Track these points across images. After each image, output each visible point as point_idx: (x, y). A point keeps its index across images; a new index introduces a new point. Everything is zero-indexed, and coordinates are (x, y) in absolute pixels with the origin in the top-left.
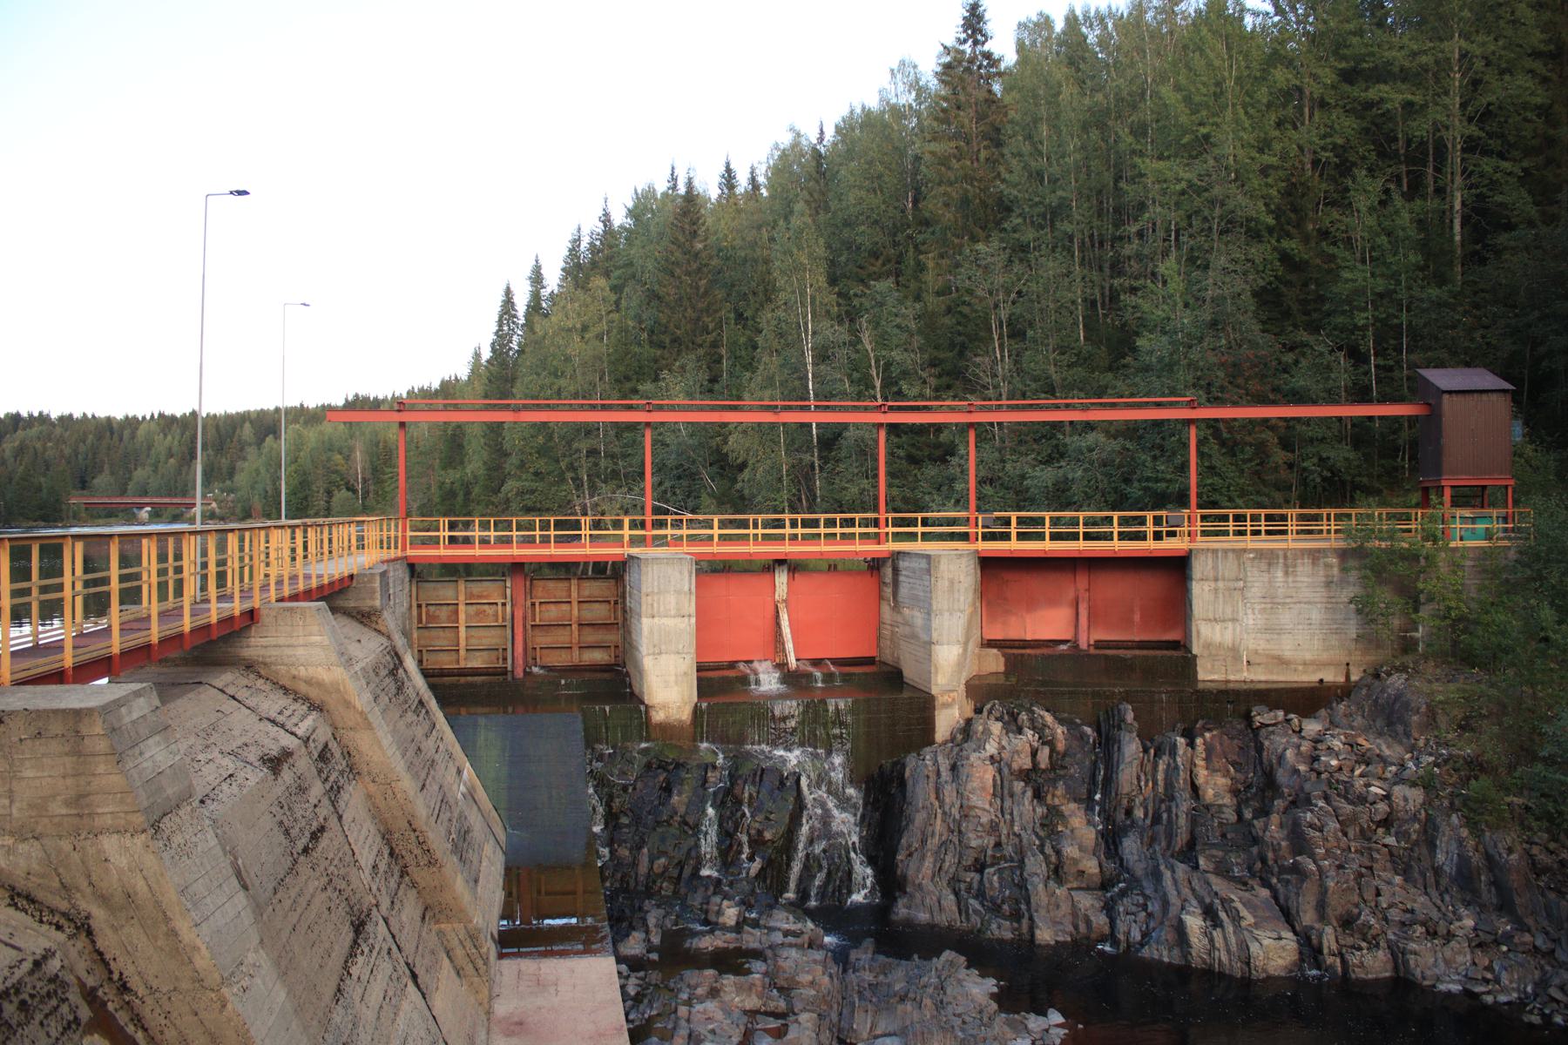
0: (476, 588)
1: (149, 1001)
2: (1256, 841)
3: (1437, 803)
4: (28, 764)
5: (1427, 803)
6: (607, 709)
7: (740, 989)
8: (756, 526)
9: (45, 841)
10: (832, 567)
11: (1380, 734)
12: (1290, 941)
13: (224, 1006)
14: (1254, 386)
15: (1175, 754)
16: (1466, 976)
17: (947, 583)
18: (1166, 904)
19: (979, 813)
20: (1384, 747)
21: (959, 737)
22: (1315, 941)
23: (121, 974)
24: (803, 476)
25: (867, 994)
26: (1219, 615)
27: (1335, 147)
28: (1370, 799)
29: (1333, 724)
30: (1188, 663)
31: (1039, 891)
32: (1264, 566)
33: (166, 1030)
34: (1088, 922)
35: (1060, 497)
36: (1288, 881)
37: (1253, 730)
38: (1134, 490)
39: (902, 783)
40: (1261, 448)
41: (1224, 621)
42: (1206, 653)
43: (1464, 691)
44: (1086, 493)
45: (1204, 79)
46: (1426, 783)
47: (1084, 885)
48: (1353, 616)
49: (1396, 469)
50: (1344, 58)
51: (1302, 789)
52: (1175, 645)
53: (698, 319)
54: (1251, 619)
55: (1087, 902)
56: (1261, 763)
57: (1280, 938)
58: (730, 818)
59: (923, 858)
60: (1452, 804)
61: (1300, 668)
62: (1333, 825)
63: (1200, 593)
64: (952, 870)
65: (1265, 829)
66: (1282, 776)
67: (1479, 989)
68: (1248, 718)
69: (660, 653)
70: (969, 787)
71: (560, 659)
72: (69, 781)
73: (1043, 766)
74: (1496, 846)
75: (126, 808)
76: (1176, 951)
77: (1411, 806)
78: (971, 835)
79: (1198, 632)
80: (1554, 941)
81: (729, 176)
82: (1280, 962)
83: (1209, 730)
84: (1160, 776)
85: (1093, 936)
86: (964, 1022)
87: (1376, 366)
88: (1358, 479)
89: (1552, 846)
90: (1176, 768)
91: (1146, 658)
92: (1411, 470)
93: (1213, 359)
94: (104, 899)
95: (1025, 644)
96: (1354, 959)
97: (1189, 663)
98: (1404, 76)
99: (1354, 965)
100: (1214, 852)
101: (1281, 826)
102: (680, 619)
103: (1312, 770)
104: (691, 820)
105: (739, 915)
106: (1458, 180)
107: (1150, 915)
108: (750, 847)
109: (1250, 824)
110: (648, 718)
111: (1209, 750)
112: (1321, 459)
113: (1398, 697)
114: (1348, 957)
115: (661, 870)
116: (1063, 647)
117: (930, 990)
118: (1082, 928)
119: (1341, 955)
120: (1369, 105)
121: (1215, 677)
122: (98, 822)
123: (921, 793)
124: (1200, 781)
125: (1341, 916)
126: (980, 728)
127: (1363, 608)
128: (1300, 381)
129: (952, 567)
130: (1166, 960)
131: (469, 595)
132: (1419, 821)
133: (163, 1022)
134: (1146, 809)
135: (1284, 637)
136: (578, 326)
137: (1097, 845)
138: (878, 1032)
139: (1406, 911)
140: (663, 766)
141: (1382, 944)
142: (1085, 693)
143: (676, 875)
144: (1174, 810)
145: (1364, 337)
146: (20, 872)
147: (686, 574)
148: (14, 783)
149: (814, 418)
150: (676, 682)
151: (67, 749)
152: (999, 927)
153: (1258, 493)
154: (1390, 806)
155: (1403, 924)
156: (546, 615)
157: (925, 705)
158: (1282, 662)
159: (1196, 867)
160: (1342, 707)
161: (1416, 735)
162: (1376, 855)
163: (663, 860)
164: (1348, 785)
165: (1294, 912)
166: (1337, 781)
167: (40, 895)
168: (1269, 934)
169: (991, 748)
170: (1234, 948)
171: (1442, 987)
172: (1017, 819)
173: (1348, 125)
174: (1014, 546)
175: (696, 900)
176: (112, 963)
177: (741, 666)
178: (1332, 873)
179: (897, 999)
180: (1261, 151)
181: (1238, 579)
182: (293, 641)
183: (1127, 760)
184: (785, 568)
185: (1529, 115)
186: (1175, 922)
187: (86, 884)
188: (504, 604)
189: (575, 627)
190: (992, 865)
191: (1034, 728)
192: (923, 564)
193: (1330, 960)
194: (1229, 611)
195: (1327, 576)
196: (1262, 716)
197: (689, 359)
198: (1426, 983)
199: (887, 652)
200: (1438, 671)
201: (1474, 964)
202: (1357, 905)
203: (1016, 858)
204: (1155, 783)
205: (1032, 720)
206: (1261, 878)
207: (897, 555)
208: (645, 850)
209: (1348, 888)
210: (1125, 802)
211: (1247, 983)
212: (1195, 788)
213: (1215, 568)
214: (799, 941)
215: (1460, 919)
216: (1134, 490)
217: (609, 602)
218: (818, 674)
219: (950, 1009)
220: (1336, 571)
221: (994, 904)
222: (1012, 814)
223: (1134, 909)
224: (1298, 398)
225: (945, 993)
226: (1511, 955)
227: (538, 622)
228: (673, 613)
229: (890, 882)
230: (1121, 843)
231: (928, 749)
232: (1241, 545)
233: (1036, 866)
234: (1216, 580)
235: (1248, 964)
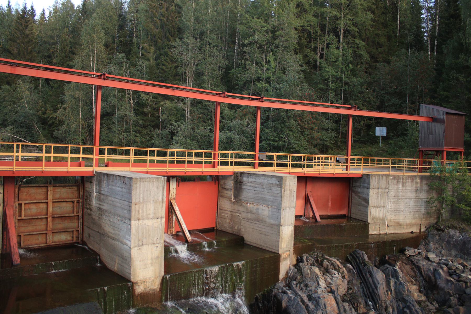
6: (106, 288)
17: (288, 192)
32: (395, 183)
41: (380, 207)
48: (423, 204)
61: (405, 227)
63: (373, 195)
71: (38, 242)
79: (370, 213)
90: (401, 283)
97: (366, 226)
102: (155, 220)
135: (401, 213)
142: (342, 246)
147: (161, 189)
150: (152, 264)
156: (29, 212)
158: (399, 225)
181: (386, 188)
184: (175, 179)
191: (335, 269)
192: (274, 181)
195: (416, 187)
213: (378, 183)
217: (73, 202)
218: (205, 244)
220: (419, 185)
227: (23, 217)
228: (152, 216)
232: (388, 173)
234: (378, 189)
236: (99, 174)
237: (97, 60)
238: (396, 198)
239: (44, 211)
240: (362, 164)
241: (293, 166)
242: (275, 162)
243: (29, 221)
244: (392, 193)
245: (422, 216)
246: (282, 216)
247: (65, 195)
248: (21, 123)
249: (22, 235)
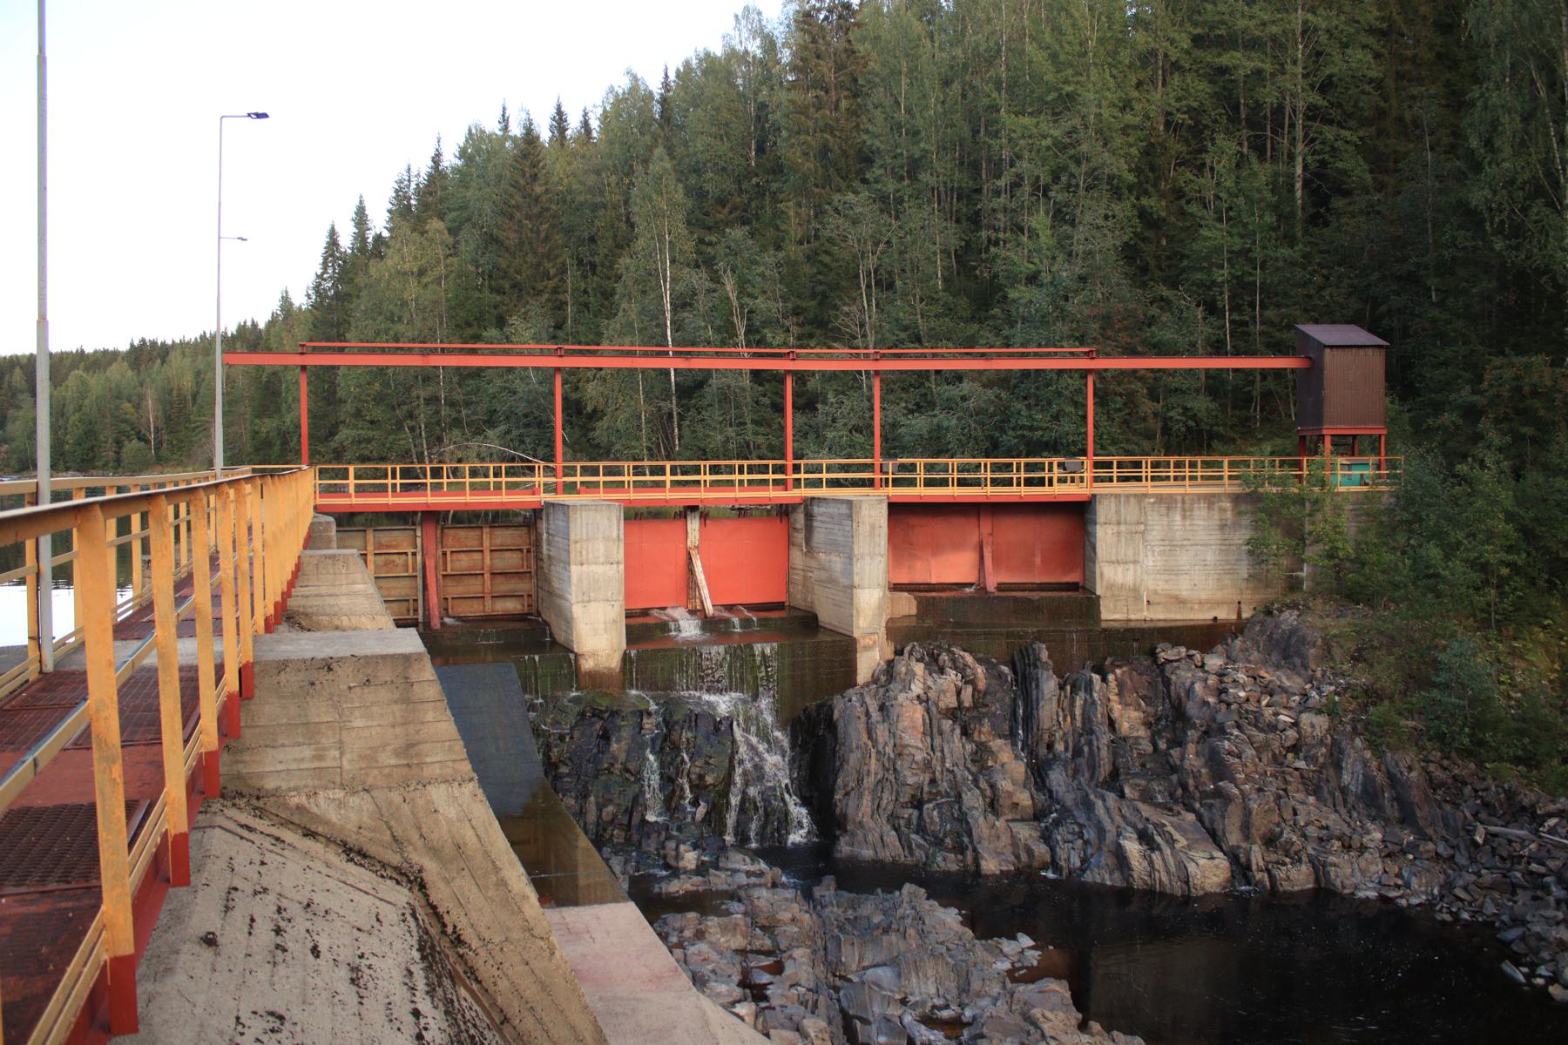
0: (385, 538)
1: (482, 952)
2: (1174, 769)
3: (1340, 728)
4: (357, 713)
5: (1332, 729)
6: (537, 658)
7: (724, 930)
8: (741, 472)
9: (375, 793)
10: (742, 512)
11: (1278, 667)
12: (1222, 862)
13: (553, 954)
14: (1123, 338)
15: (1091, 690)
16: (1380, 883)
17: (868, 528)
18: (1101, 831)
19: (913, 751)
20: (1284, 679)
21: (883, 678)
22: (1243, 860)
23: (455, 927)
24: (662, 422)
25: (848, 927)
26: (1121, 556)
27: (1190, 110)
28: (1281, 726)
29: (1230, 659)
30: (1091, 604)
31: (981, 824)
32: (1163, 511)
33: (499, 982)
34: (1029, 851)
35: (936, 445)
36: (1211, 806)
37: (1158, 666)
38: (1009, 438)
39: (832, 726)
40: (1131, 399)
41: (1126, 563)
42: (1108, 595)
43: (1355, 625)
44: (960, 440)
45: (1071, 38)
46: (1330, 711)
47: (1018, 817)
48: (1244, 557)
49: (1247, 419)
50: (1196, 25)
51: (1214, 720)
52: (1073, 587)
53: (539, 264)
54: (1151, 561)
55: (1025, 832)
56: (1169, 696)
57: (1212, 858)
58: (670, 764)
59: (861, 797)
60: (1354, 729)
61: (1196, 607)
62: (1250, 752)
63: (1105, 536)
64: (890, 807)
65: (1182, 758)
66: (1192, 709)
67: (1392, 894)
68: (1152, 654)
69: (589, 601)
70: (900, 726)
71: (473, 609)
72: (398, 730)
73: (966, 704)
74: (1397, 765)
75: (454, 757)
76: (1117, 875)
77: (1317, 732)
78: (907, 773)
79: (1102, 574)
80: (1453, 847)
81: (561, 118)
82: (1215, 879)
83: (1119, 667)
84: (1078, 712)
85: (1035, 864)
86: (948, 949)
87: (1231, 322)
88: (1215, 428)
89: (1445, 763)
90: (1094, 702)
91: (1053, 599)
92: (1262, 421)
93: (1086, 312)
94: (435, 851)
95: (930, 587)
96: (1280, 873)
97: (1092, 603)
98: (1253, 44)
99: (1281, 879)
100: (1138, 781)
101: (1197, 754)
102: (608, 567)
103: (1221, 701)
104: (632, 766)
105: (698, 859)
106: (1300, 147)
107: (1086, 842)
108: (691, 791)
109: (1166, 754)
110: (578, 666)
111: (1121, 685)
112: (1186, 409)
113: (1293, 632)
114: (1275, 872)
115: (610, 818)
116: (968, 590)
117: (909, 921)
118: (1024, 857)
119: (1269, 872)
120: (1223, 71)
121: (1117, 616)
122: (427, 772)
123: (854, 734)
124: (1116, 715)
125: (1265, 834)
126: (903, 669)
127: (1256, 550)
128: (1167, 335)
129: (872, 512)
130: (1108, 883)
131: (378, 545)
132: (1326, 746)
133: (496, 973)
134: (1066, 743)
135: (1181, 577)
136: (415, 270)
137: (1027, 778)
138: (866, 963)
139: (1322, 828)
140: (597, 714)
141: (1304, 858)
143: (626, 822)
144: (1095, 743)
145: (1221, 293)
146: (351, 827)
147: (615, 521)
148: (344, 732)
149: (672, 364)
150: (605, 630)
151: (396, 696)
152: (944, 860)
153: (1128, 441)
154: (1299, 732)
155: (1321, 839)
156: (457, 565)
157: (846, 648)
158: (1180, 601)
159: (1122, 796)
160: (1238, 642)
161: (1313, 667)
162: (1289, 778)
163: (611, 808)
164: (1258, 715)
165: (1220, 833)
166: (1247, 711)
167: (372, 850)
168: (1202, 854)
169: (917, 688)
170: (1173, 869)
171: (1361, 894)
172: (948, 755)
173: (1202, 88)
174: (920, 492)
175: (651, 846)
176: (445, 916)
177: (655, 613)
178: (1254, 796)
179: (880, 931)
180: (1123, 109)
181: (1139, 523)
182: (336, 590)
183: (1047, 697)
185: (1367, 88)
186: (1112, 848)
187: (417, 837)
188: (414, 554)
189: (487, 576)
190: (930, 801)
191: (956, 668)
192: (844, 509)
193: (1258, 876)
194: (1130, 553)
195: (1221, 520)
196: (1166, 653)
197: (535, 306)
198: (1346, 891)
199: (799, 596)
200: (1327, 607)
201: (1386, 872)
202: (1278, 825)
203: (952, 794)
204: (1073, 718)
205: (954, 661)
206: (1185, 805)
207: (809, 502)
208: (592, 799)
209: (1269, 809)
210: (1046, 737)
211: (1187, 900)
212: (1112, 724)
213: (1118, 512)
214: (762, 881)
215: (1368, 833)
216: (1009, 438)
217: (521, 550)
218: (736, 620)
219: (932, 937)
220: (1229, 515)
221: (936, 837)
222: (942, 751)
223: (1070, 837)
224: (1160, 350)
225: (924, 923)
226: (1417, 862)
227: (449, 572)
228: (601, 560)
229: (829, 821)
230: (1047, 775)
231: (851, 691)
232: (1143, 490)
233: (973, 800)
234: (1119, 523)
235: (1187, 883)
236: (550, 505)
237: (673, 261)
238: (1167, 543)
239: (480, 563)
240: (1226, 473)
241: (995, 482)
242: (921, 475)
243: (459, 577)
244: (1154, 533)
245: (1244, 584)
246: (855, 570)
247: (509, 541)
248: (526, 416)
249: (449, 597)
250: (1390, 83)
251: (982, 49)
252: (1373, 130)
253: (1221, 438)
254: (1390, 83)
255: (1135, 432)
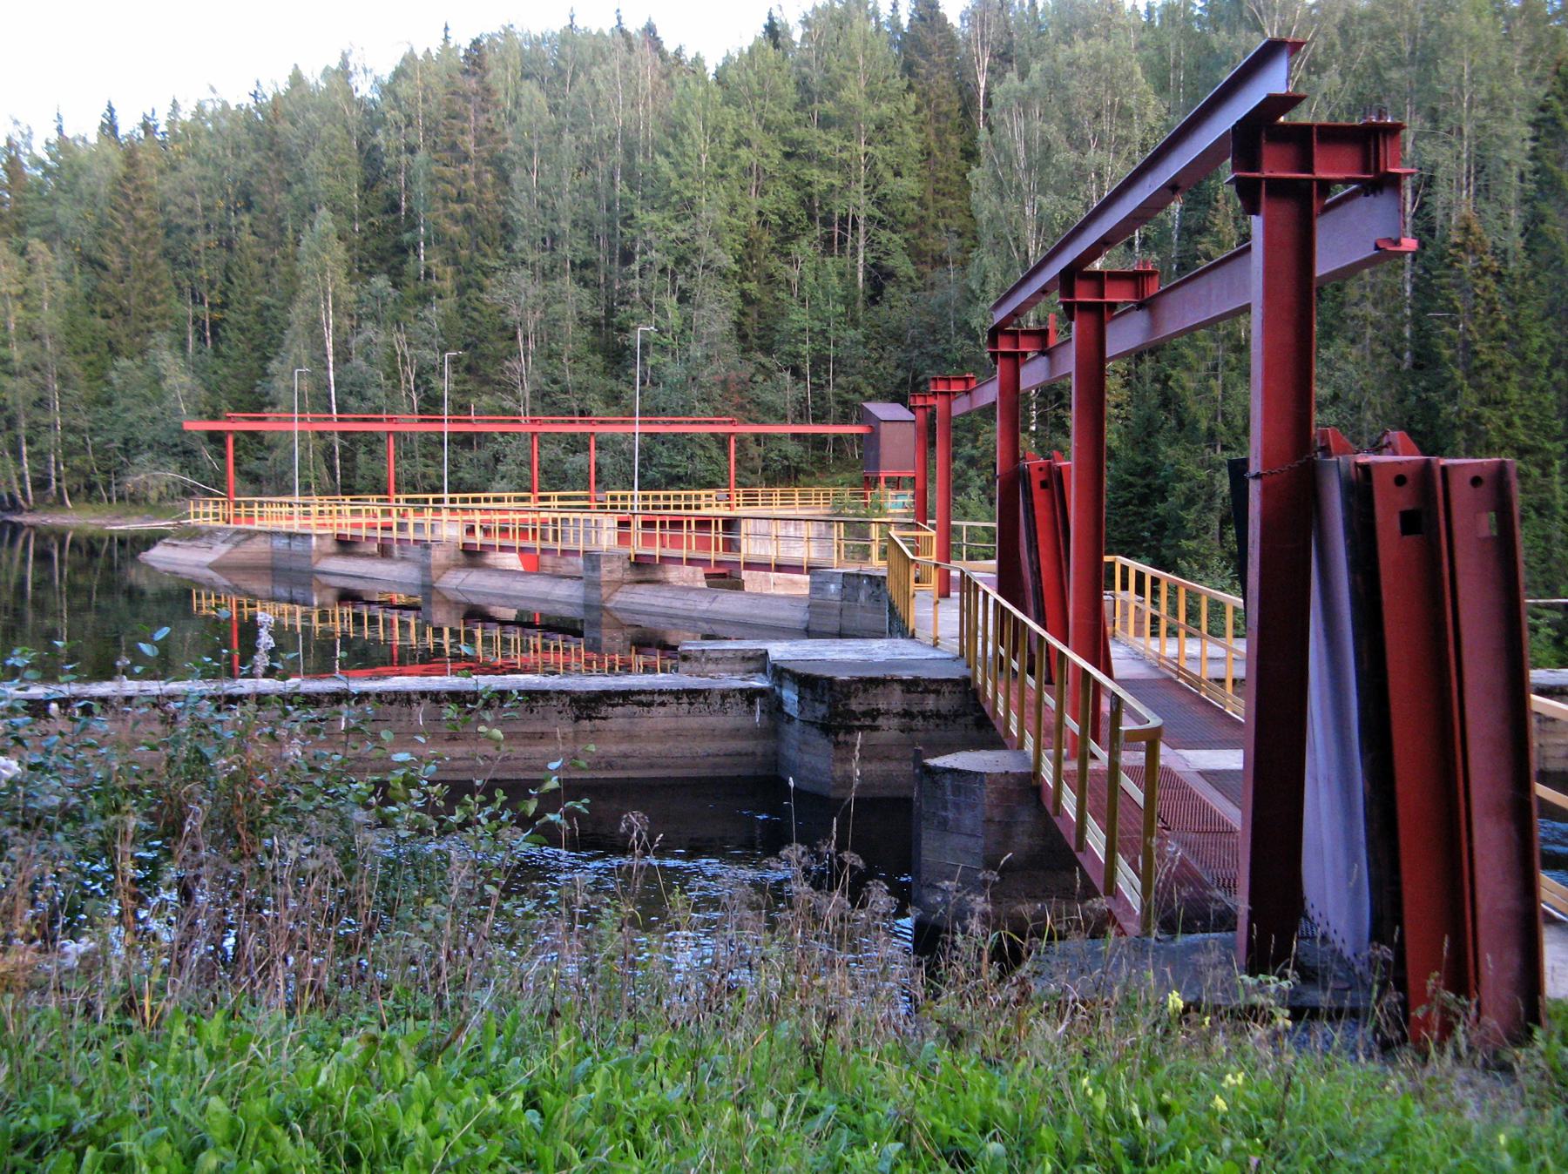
53: (146, 290)
98: (826, 164)
128: (769, 397)
180: (730, 214)
250: (929, 197)
251: (606, 136)
252: (916, 232)
253: (804, 472)
254: (929, 197)
255: (745, 468)
